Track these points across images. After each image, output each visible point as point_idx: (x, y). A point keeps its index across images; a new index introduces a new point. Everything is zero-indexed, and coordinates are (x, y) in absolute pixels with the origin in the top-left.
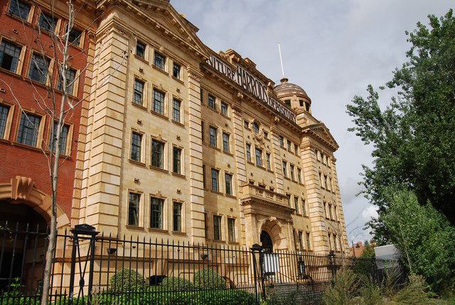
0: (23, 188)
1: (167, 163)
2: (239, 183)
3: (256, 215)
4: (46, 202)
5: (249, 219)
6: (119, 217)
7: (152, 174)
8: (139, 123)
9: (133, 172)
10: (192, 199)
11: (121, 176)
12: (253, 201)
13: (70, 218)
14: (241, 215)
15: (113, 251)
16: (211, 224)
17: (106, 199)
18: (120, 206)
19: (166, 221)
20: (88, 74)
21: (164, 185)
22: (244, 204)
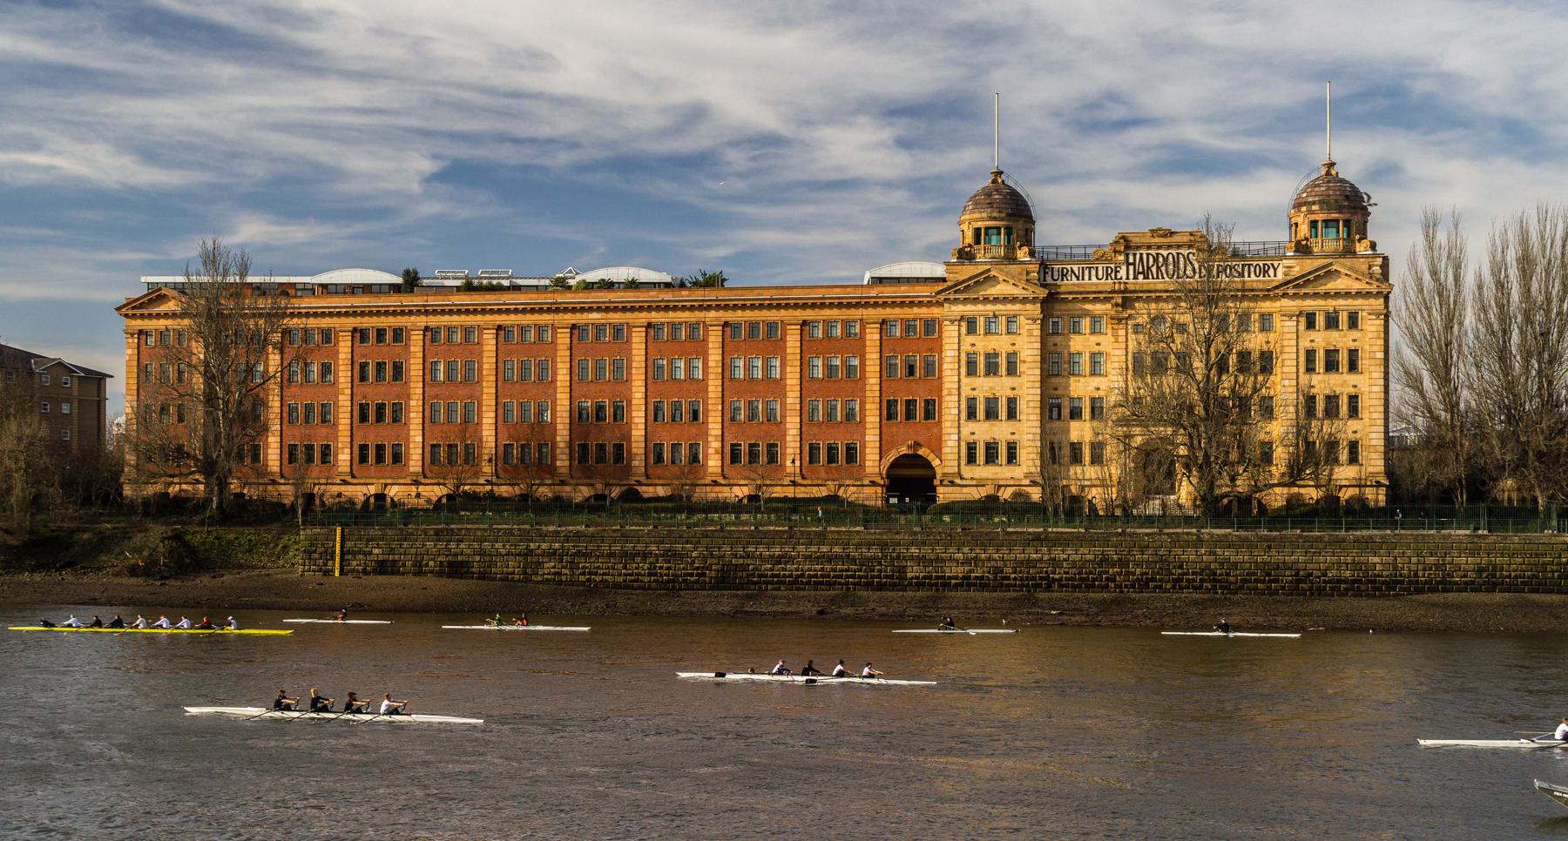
1: (1003, 413)
7: (987, 424)
8: (974, 389)
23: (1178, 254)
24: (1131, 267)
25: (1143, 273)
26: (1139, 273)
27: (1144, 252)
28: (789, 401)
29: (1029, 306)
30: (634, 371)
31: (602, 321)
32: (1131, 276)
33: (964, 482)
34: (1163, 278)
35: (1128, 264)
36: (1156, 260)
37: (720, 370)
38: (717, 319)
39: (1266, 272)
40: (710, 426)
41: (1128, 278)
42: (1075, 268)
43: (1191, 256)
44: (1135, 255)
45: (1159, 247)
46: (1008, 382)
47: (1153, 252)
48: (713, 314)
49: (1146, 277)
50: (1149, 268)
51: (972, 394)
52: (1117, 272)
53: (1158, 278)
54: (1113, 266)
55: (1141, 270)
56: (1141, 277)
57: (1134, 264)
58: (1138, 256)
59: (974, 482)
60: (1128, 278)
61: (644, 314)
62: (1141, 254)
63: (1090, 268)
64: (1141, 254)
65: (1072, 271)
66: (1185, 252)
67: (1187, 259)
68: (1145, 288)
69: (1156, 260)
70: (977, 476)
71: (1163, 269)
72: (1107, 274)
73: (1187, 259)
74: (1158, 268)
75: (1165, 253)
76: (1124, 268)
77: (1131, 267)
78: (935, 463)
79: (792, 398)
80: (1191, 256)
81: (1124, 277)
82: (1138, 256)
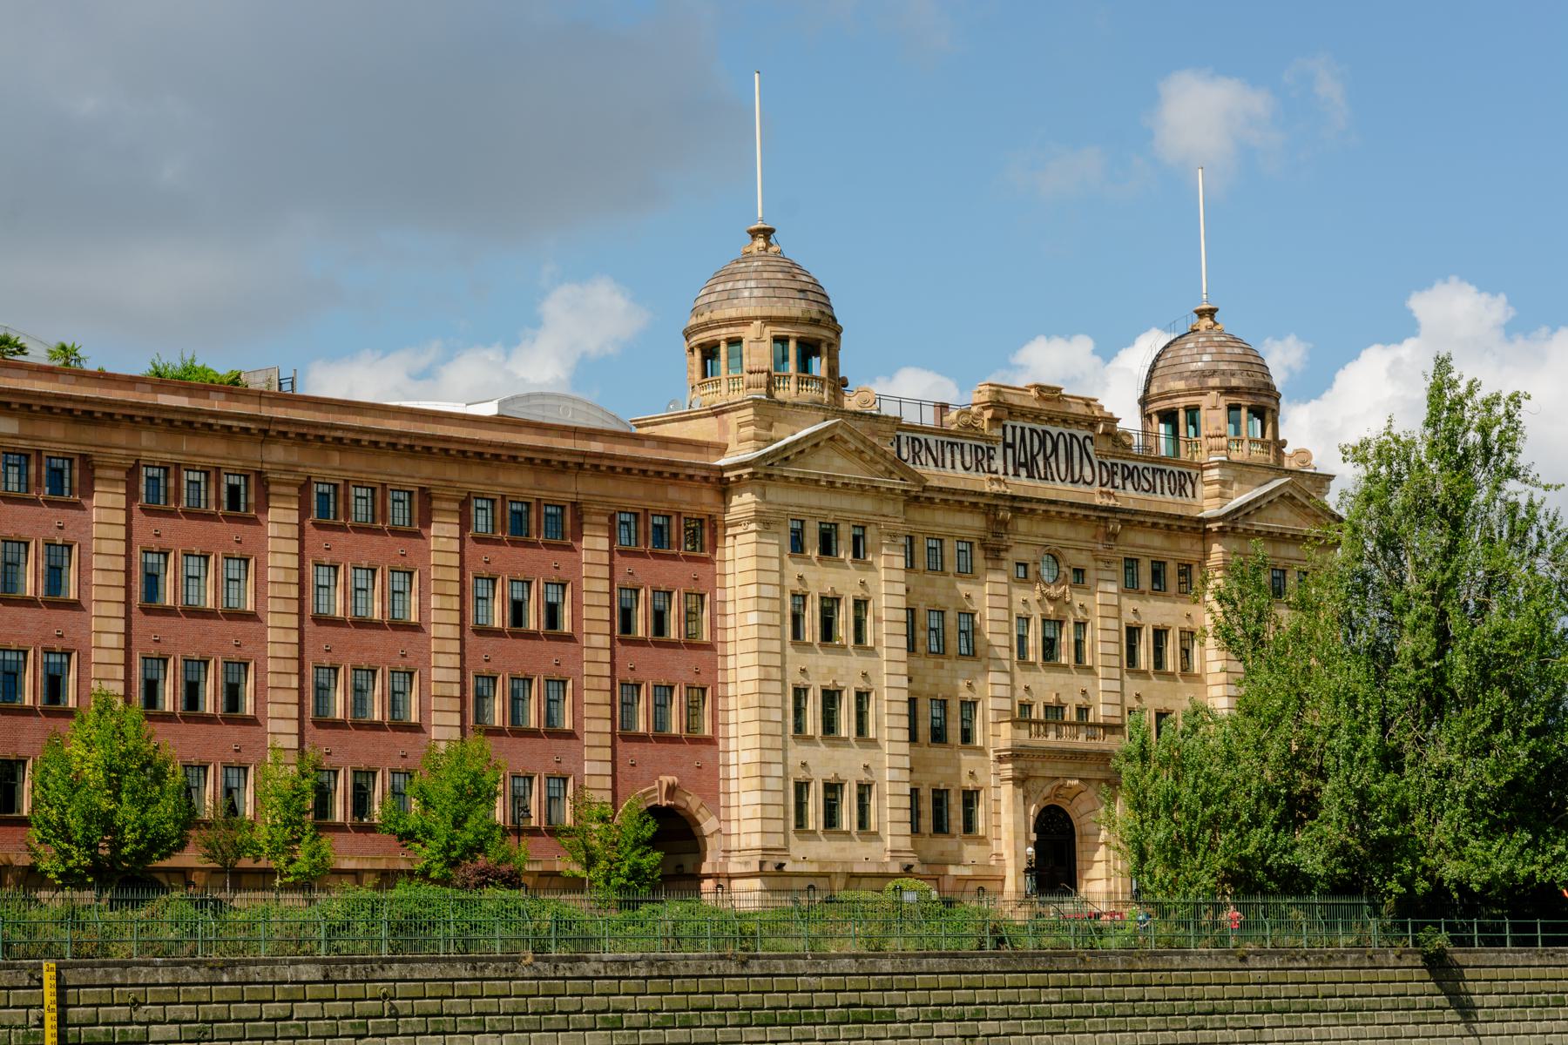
0: (672, 790)
2: (991, 716)
3: (1020, 781)
4: (692, 802)
5: (1007, 790)
6: (786, 820)
7: (823, 750)
9: (797, 753)
10: (887, 775)
11: (785, 763)
12: (1016, 754)
13: (720, 821)
14: (993, 781)
15: (780, 866)
16: (927, 807)
17: (769, 798)
18: (785, 806)
19: (847, 817)
20: (719, 595)
21: (846, 763)
22: (1000, 760)
23: (1072, 436)
24: (1010, 451)
25: (1024, 465)
26: (1021, 465)
27: (1027, 426)
28: (436, 674)
29: (888, 509)
30: (96, 578)
31: (22, 443)
32: (1011, 470)
33: (799, 868)
34: (1053, 480)
35: (1006, 445)
36: (1042, 443)
37: (294, 592)
38: (289, 468)
39: (1183, 488)
40: (271, 726)
41: (1006, 473)
42: (932, 440)
43: (1088, 441)
44: (1014, 428)
45: (1050, 420)
46: (856, 662)
47: (1039, 427)
48: (277, 454)
49: (1030, 476)
50: (1033, 457)
51: (801, 681)
52: (991, 458)
53: (1046, 479)
54: (984, 445)
55: (1022, 460)
56: (1023, 472)
57: (1012, 446)
58: (1018, 432)
59: (814, 868)
60: (1006, 473)
61: (120, 437)
62: (1023, 429)
63: (952, 444)
64: (1023, 429)
65: (928, 449)
66: (1081, 434)
67: (1083, 448)
68: (1030, 494)
69: (1042, 443)
70: (811, 855)
71: (1052, 459)
72: (979, 462)
73: (1083, 448)
74: (1046, 459)
75: (1054, 431)
76: (1000, 449)
77: (1010, 451)
78: (708, 825)
79: (443, 670)
80: (1088, 441)
81: (1001, 471)
82: (1018, 432)
